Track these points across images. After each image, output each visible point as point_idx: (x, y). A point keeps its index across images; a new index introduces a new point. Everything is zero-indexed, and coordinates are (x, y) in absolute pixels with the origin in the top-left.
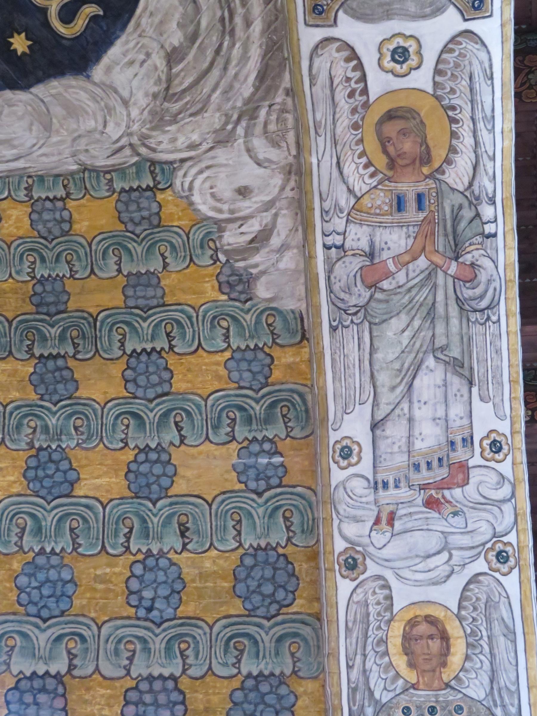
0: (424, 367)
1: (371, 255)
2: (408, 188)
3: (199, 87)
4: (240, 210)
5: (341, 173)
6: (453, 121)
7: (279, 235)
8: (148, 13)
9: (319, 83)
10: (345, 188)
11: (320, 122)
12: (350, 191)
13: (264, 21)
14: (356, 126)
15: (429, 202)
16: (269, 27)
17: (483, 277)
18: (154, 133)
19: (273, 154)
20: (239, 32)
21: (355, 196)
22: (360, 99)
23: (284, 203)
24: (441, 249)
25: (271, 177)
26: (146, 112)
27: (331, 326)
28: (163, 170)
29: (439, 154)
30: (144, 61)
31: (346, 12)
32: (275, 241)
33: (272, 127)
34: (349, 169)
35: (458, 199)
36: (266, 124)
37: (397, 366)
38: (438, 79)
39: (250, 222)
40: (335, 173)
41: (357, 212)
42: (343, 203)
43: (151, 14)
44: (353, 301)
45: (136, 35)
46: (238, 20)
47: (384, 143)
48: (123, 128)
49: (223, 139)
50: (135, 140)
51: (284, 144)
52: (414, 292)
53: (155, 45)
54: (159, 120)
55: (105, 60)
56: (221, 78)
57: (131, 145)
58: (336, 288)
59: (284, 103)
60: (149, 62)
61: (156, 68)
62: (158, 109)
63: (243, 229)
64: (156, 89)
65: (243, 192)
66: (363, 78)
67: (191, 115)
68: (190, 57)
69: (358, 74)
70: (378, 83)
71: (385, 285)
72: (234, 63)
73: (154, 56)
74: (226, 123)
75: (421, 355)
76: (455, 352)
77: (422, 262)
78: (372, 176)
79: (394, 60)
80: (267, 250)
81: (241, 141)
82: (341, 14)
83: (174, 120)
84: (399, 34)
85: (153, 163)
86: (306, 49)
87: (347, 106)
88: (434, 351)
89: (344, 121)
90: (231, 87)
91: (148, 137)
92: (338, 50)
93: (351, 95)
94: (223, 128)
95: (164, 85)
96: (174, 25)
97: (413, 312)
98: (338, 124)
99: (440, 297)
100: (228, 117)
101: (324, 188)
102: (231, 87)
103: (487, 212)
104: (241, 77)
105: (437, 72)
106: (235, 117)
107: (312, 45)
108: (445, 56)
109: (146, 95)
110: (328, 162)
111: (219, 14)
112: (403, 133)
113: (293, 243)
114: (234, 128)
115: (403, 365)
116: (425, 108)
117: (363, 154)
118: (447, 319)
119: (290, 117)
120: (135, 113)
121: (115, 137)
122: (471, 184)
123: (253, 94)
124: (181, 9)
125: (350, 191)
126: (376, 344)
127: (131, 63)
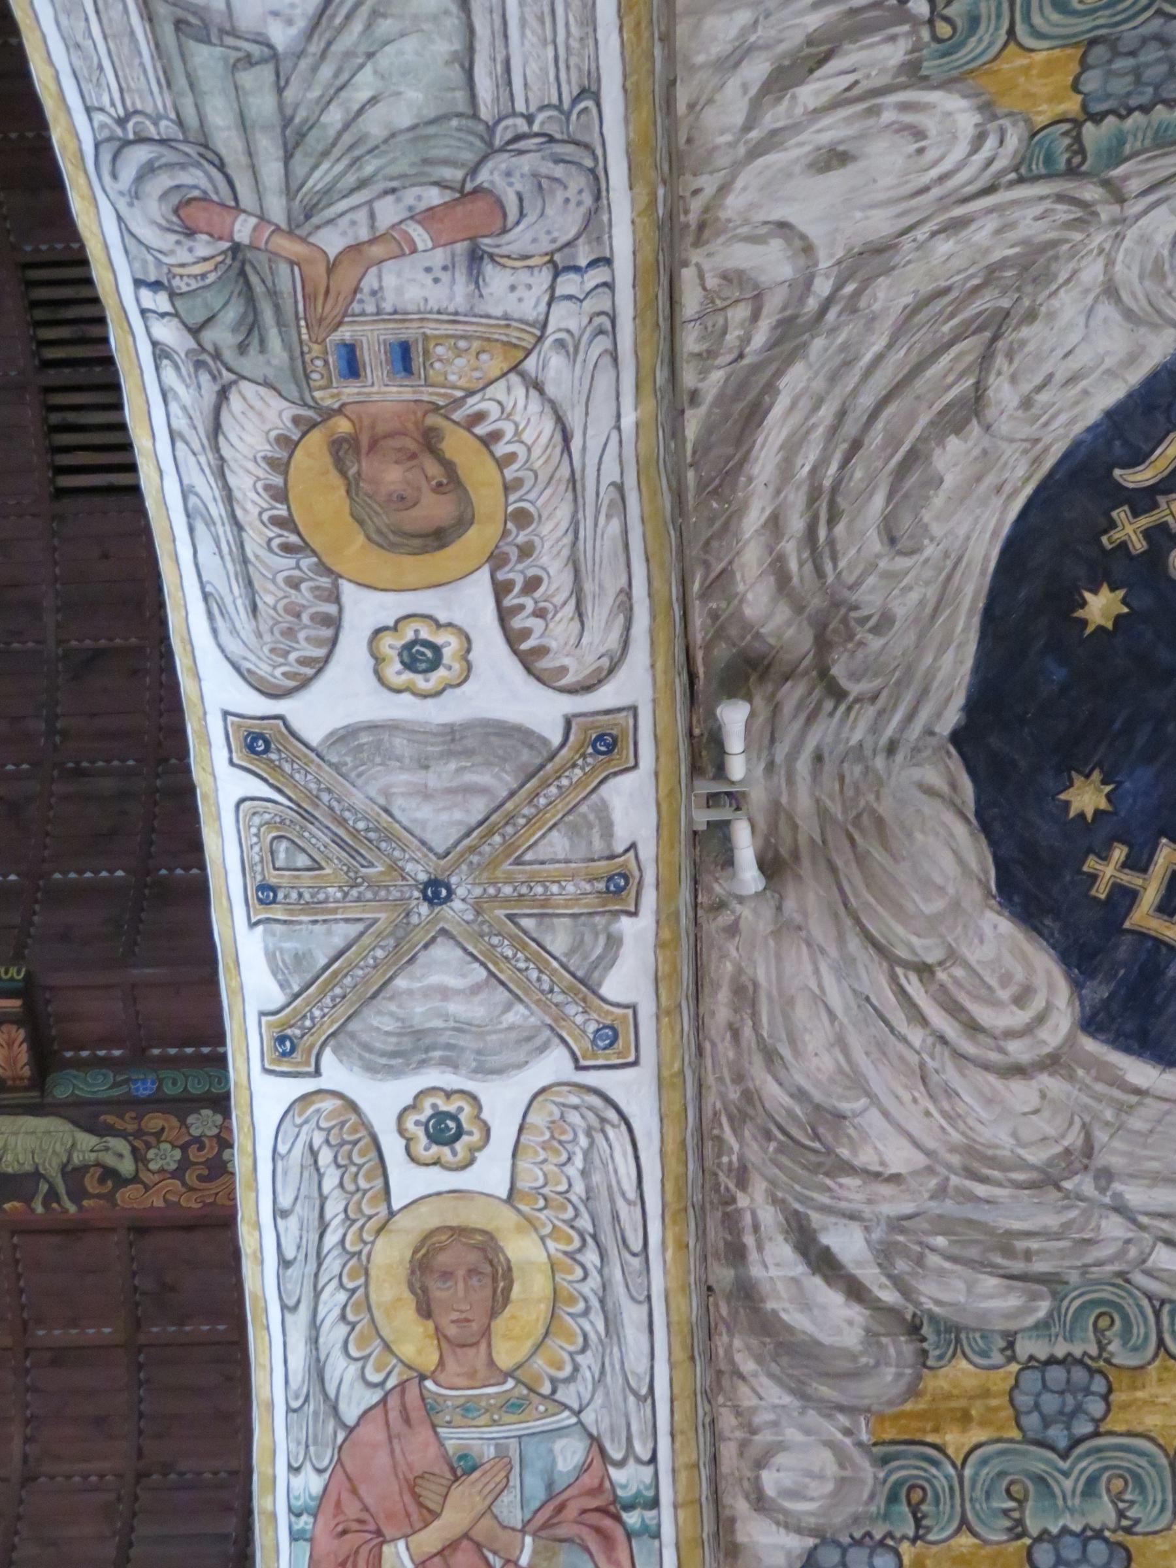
0: (301, 24)
1: (476, 258)
2: (383, 392)
3: (914, 358)
4: (848, 120)
5: (560, 420)
6: (286, 523)
7: (745, 87)
8: (1008, 489)
9: (609, 600)
10: (550, 390)
11: (609, 517)
12: (536, 386)
13: (737, 535)
14: (522, 518)
15: (323, 360)
16: (726, 527)
17: (155, 208)
18: (1053, 235)
19: (740, 256)
20: (796, 499)
21: (523, 375)
22: (514, 574)
23: (723, 160)
24: (283, 268)
25: (752, 206)
26: (1063, 276)
27: (597, 98)
28: (1049, 160)
29: (313, 452)
30: (1039, 389)
31: (545, 741)
32: (757, 70)
33: (741, 312)
34: (538, 429)
35: (250, 364)
36: (755, 316)
37: (385, 27)
38: (332, 609)
39: (824, 99)
40: (575, 420)
41: (518, 348)
42: (557, 361)
43: (999, 489)
44: (526, 163)
45: (1047, 440)
46: (796, 524)
47: (452, 481)
48: (1132, 233)
49: (873, 258)
50: (1106, 212)
51: (712, 282)
52: (351, 179)
53: (1004, 427)
54: (1034, 267)
55: (1135, 377)
56: (855, 392)
57: (1121, 200)
58: (577, 182)
59: (704, 373)
60: (1026, 387)
61: (1014, 379)
62: (1029, 289)
63: (849, 79)
64: (1025, 332)
65: (835, 158)
66: (504, 616)
67: (947, 290)
68: (924, 420)
69: (517, 623)
70: (471, 604)
71: (434, 197)
72: (818, 434)
73: (1015, 403)
74: (857, 294)
75: (315, 48)
76: (205, 57)
77: (332, 242)
78: (480, 417)
79: (437, 649)
80: (781, 48)
81: (824, 264)
82: (556, 739)
83: (992, 273)
84: (425, 696)
85: (1072, 172)
86: (640, 654)
87: (544, 560)
88: (274, 56)
89: (551, 533)
90: (834, 378)
91: (1069, 225)
92: (563, 670)
93: (532, 584)
94: (866, 283)
95: (1000, 344)
96: (949, 481)
97: (347, 139)
98: (565, 524)
99: (272, 170)
100: (852, 308)
101: (605, 381)
102: (834, 378)
103: (168, 333)
104: (805, 404)
105: (334, 623)
106: (831, 316)
107: (622, 674)
108: (321, 652)
109: (1051, 316)
110: (593, 437)
111: (840, 529)
112: (402, 501)
113: (702, 75)
114: (838, 288)
115: (369, 26)
116: (354, 552)
117: (503, 463)
118: (243, 123)
119: (691, 341)
120: (1092, 272)
121: (1163, 210)
122: (223, 394)
123: (779, 374)
124: (927, 516)
125: (536, 386)
126: (455, 74)
127: (1072, 380)
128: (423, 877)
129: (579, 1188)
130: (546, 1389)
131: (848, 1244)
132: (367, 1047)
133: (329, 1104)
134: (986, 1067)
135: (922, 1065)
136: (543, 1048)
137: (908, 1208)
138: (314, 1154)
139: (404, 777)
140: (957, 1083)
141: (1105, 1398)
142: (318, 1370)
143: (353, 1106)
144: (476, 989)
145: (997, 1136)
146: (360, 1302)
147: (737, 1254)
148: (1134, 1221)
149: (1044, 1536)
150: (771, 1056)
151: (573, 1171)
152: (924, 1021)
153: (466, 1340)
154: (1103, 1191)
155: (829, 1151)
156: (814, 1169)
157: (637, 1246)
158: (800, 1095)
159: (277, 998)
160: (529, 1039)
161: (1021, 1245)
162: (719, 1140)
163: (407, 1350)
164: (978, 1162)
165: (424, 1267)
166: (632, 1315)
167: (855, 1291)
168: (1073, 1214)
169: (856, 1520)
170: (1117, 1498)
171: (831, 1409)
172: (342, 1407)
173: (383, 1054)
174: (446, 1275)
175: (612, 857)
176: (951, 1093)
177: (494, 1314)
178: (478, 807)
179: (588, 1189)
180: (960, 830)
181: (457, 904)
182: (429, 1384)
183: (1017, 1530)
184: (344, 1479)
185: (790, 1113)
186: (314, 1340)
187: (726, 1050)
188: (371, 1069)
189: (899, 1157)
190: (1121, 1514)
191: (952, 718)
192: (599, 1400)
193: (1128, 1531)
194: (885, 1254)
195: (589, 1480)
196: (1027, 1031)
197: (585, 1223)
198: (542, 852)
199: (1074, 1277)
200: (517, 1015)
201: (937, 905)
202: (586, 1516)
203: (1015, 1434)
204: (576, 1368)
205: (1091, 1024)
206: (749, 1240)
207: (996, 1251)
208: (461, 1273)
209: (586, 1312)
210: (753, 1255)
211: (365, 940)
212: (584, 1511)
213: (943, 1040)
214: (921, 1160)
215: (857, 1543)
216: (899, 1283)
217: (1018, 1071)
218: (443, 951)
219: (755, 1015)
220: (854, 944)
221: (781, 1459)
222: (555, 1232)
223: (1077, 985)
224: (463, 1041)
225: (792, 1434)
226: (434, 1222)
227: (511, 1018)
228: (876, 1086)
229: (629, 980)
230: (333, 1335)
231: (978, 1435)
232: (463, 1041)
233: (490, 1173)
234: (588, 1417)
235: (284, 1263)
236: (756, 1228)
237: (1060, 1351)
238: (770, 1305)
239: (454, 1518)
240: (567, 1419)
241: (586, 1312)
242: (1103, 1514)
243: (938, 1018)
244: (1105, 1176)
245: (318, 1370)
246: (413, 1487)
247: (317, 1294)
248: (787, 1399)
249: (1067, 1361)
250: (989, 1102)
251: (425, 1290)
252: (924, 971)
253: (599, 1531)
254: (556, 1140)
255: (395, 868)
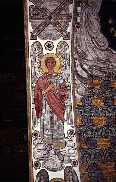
128: (49, 16)
129: (63, 53)
130: (59, 75)
131: (86, 67)
132: (42, 36)
133: (37, 43)
134: (100, 49)
135: (94, 48)
136: (61, 37)
137: (92, 64)
138: (35, 49)
139: (48, 3)
140: (97, 51)
141: (111, 84)
142: (35, 72)
143: (40, 43)
144: (54, 30)
145: (101, 57)
146: (40, 66)
147: (75, 67)
148: (113, 67)
149: (105, 97)
150: (79, 46)
151: (62, 51)
152: (94, 44)
153: (51, 69)
154: (110, 64)
155: (84, 57)
156: (83, 59)
157: (69, 60)
158: (82, 51)
159: (32, 30)
160: (59, 36)
161: (102, 69)
162: (74, 55)
163: (45, 71)
164: (99, 59)
165: (47, 62)
166: (68, 67)
167: (87, 72)
168: (107, 66)
169: (87, 94)
170: (112, 94)
171: (84, 84)
172: (38, 77)
173: (43, 37)
174: (49, 62)
175: (69, 14)
176: (96, 52)
177: (54, 66)
178: (56, 7)
179: (64, 53)
180: (98, 23)
181: (52, 20)
182: (47, 74)
183: (103, 96)
184: (38, 84)
185: (81, 52)
186: (35, 70)
187: (75, 44)
188: (42, 39)
189: (91, 59)
190: (113, 95)
191: (98, 12)
192: (65, 76)
193: (113, 97)
194: (90, 68)
195: (63, 84)
196: (103, 46)
197: (64, 57)
198: (62, 13)
199: (107, 72)
200: (58, 33)
201: (95, 32)
202: (63, 88)
203: (102, 87)
204: (62, 72)
205: (109, 46)
206: (76, 66)
207: (100, 69)
208: (50, 62)
209: (64, 66)
210: (77, 67)
211: (42, 23)
212: (63, 87)
213: (96, 46)
214: (93, 59)
215: (87, 97)
216: (91, 71)
217: (102, 50)
218: (51, 25)
219: (78, 41)
220: (88, 35)
221: (80, 88)
222: (60, 58)
223: (108, 42)
224: (52, 36)
225: (81, 86)
226: (48, 57)
227: (57, 33)
228: (89, 51)
229: (69, 30)
230: (37, 69)
231: (98, 87)
232: (52, 36)
233: (54, 51)
234: (63, 78)
235: (32, 61)
236: (77, 64)
237: (106, 79)
238: (79, 73)
239: (49, 88)
240: (61, 78)
241: (64, 66)
242: (111, 95)
243: (95, 43)
244: (111, 62)
245: (35, 72)
246: (45, 85)
247: (35, 64)
248: (80, 82)
249: (107, 80)
250: (100, 53)
251: (47, 64)
252: (94, 38)
253: (65, 89)
254: (61, 48)
255: (46, 15)
